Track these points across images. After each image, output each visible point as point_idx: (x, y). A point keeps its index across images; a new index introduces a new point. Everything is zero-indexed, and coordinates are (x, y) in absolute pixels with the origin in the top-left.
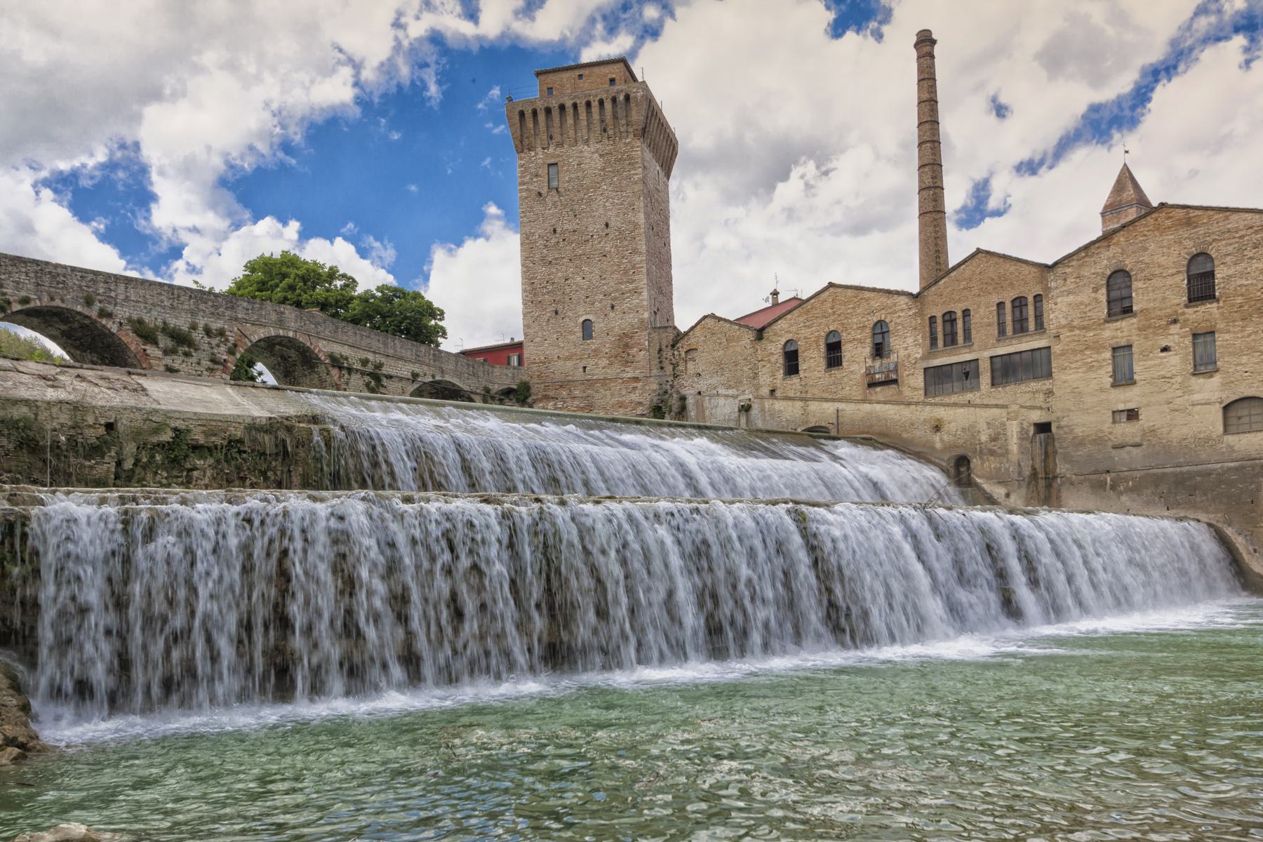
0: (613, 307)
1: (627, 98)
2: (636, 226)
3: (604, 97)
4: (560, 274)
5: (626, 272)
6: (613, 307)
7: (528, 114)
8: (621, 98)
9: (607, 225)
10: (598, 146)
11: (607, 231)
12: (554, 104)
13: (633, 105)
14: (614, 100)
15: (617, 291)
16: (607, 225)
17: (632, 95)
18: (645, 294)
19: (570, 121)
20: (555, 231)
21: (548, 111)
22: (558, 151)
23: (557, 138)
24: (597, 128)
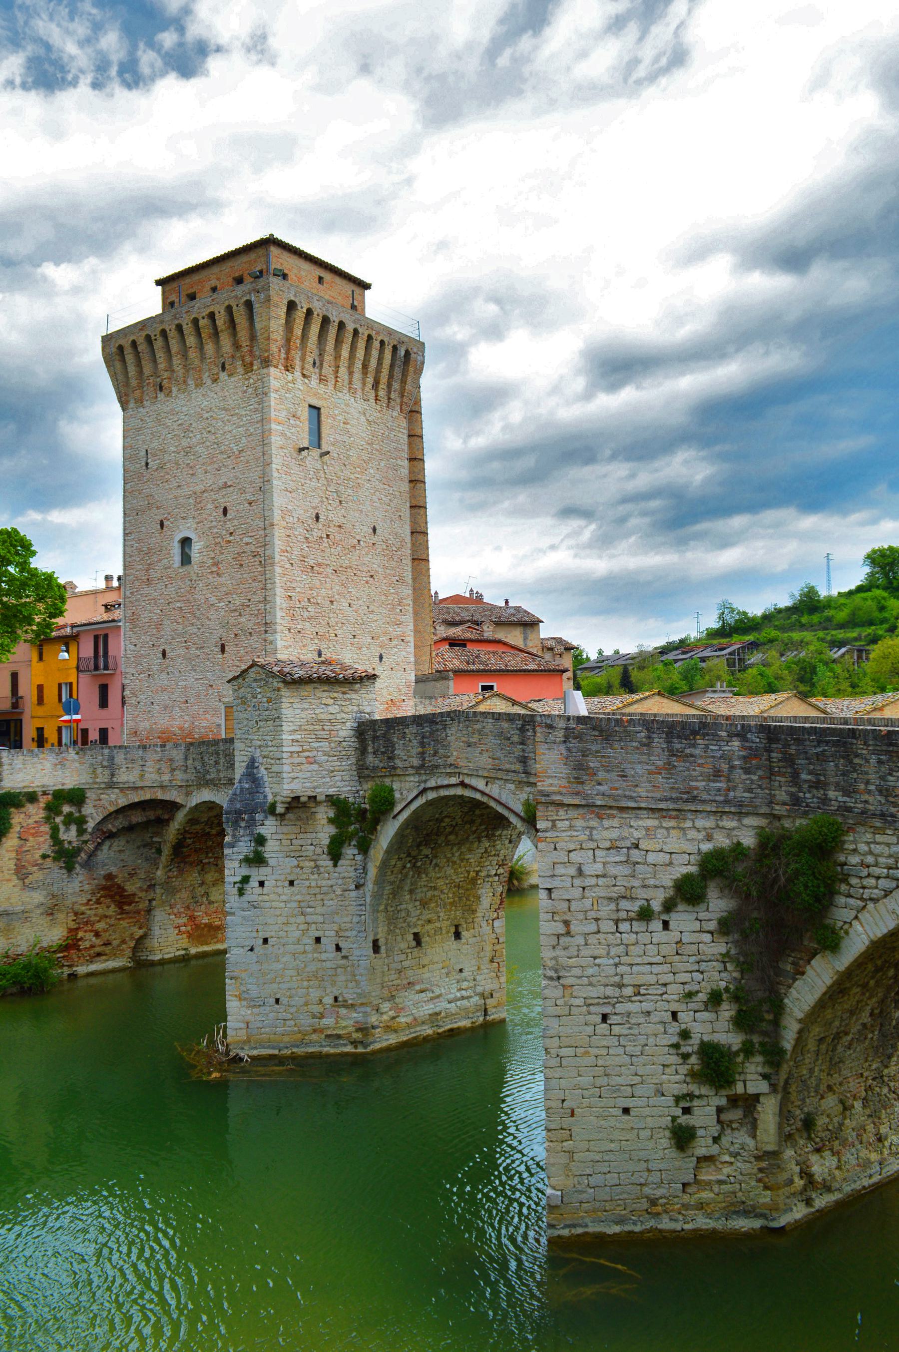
0: (381, 658)
1: (407, 353)
2: (403, 541)
3: (386, 340)
4: (323, 592)
5: (393, 609)
6: (381, 658)
7: (300, 314)
8: (403, 353)
9: (374, 530)
10: (365, 405)
11: (375, 539)
12: (335, 318)
13: (411, 369)
14: (395, 348)
15: (385, 633)
16: (374, 530)
17: (413, 355)
18: (412, 644)
19: (345, 353)
20: (317, 518)
21: (326, 321)
22: (322, 389)
23: (328, 370)
24: (370, 380)
